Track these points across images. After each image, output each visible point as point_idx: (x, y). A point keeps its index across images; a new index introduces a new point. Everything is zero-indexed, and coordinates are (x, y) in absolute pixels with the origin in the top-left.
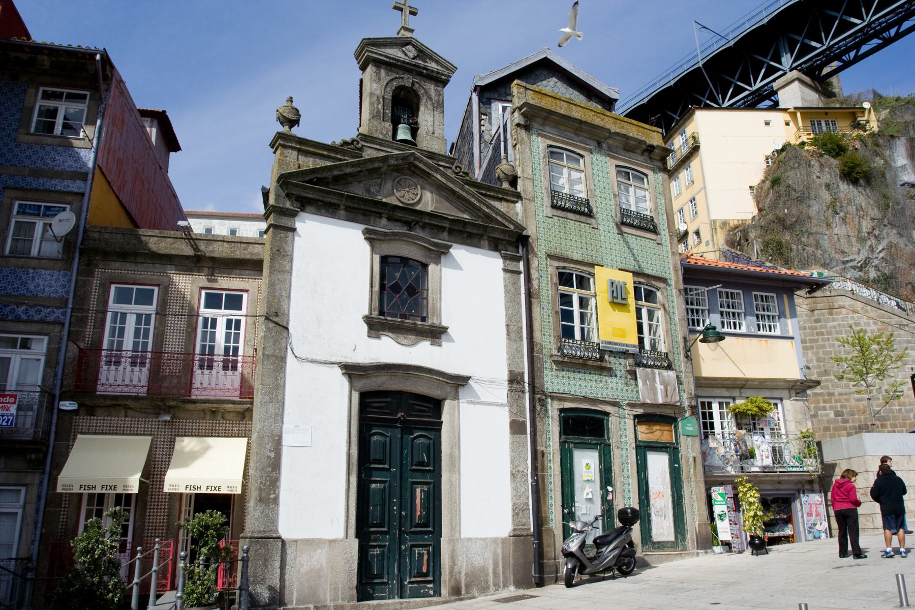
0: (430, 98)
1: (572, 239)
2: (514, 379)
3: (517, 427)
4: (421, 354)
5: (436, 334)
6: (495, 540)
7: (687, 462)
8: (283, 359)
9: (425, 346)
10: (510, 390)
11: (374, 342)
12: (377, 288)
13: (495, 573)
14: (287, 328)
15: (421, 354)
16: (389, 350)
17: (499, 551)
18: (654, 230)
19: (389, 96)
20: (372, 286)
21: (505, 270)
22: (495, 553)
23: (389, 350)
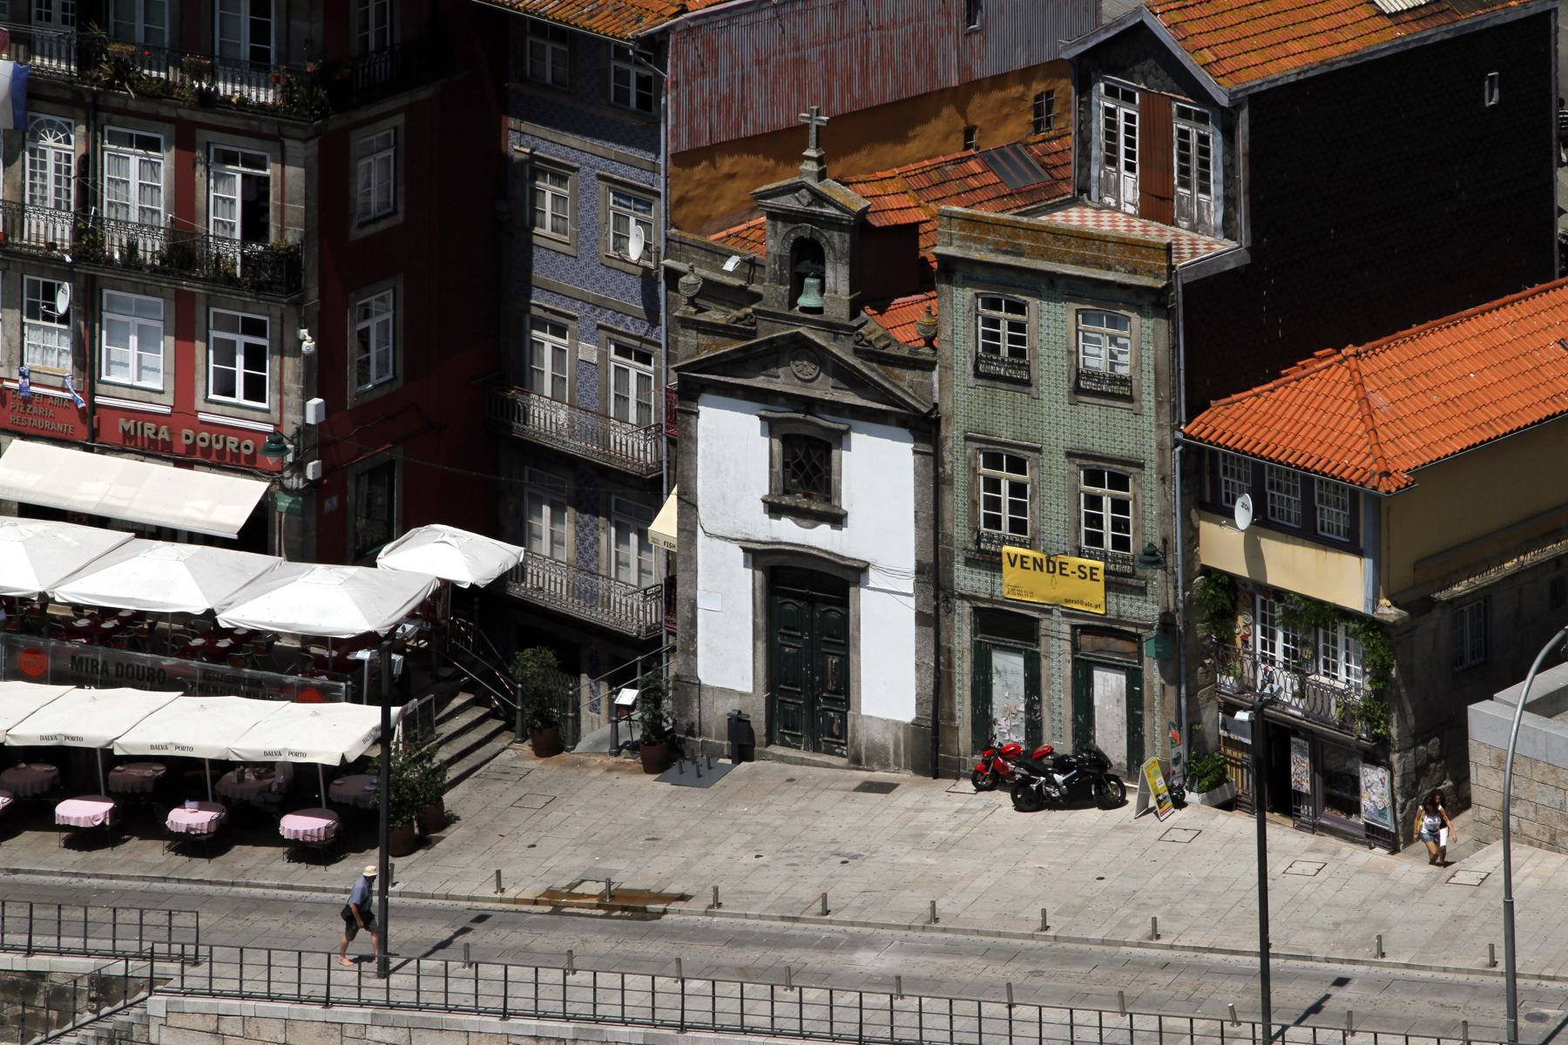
0: (832, 248)
1: (1004, 417)
2: (920, 569)
3: (921, 618)
4: (820, 537)
5: (837, 520)
6: (897, 723)
7: (1151, 687)
8: (694, 534)
9: (825, 528)
10: (917, 581)
11: (774, 521)
12: (778, 467)
13: (896, 753)
14: (696, 506)
15: (820, 537)
16: (788, 531)
17: (901, 735)
18: (1129, 399)
19: (787, 252)
20: (771, 466)
21: (915, 452)
22: (896, 736)
23: (788, 531)
